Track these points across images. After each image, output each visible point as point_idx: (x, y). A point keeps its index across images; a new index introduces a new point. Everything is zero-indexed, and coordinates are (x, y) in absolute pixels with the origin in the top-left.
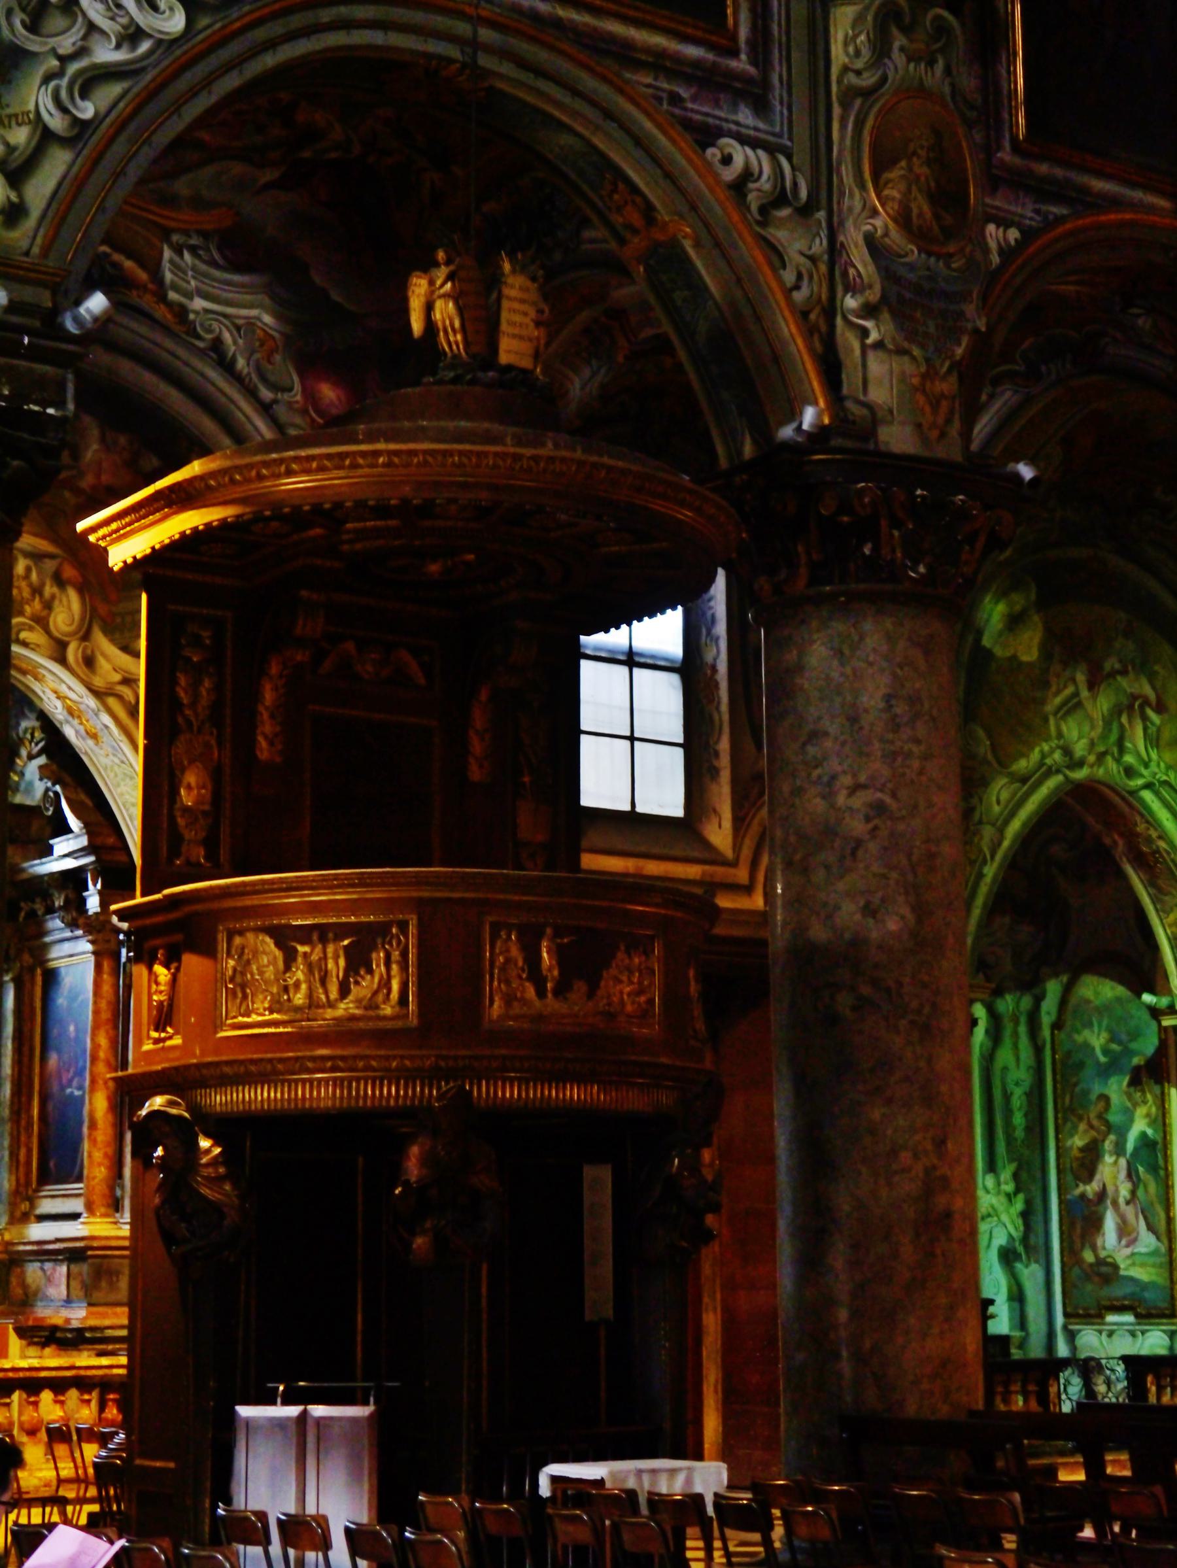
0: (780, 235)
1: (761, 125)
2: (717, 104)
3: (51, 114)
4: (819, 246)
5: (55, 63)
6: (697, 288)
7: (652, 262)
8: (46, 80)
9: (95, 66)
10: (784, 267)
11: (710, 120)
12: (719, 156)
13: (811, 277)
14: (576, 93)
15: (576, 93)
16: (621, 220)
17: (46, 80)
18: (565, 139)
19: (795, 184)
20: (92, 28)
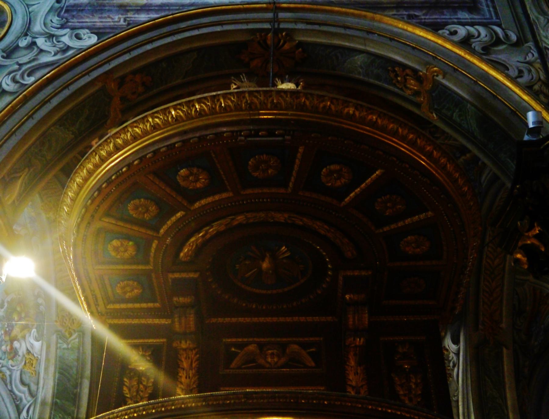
0: (502, 57)
1: (475, 17)
2: (443, 14)
3: (8, 85)
4: (533, 56)
5: (16, 67)
6: (459, 102)
7: (436, 107)
8: (9, 74)
9: (40, 64)
10: (508, 69)
11: (439, 20)
12: (448, 32)
13: (530, 71)
14: (346, 27)
15: (346, 27)
16: (409, 92)
17: (9, 74)
18: (359, 59)
19: (507, 36)
20: (41, 51)
